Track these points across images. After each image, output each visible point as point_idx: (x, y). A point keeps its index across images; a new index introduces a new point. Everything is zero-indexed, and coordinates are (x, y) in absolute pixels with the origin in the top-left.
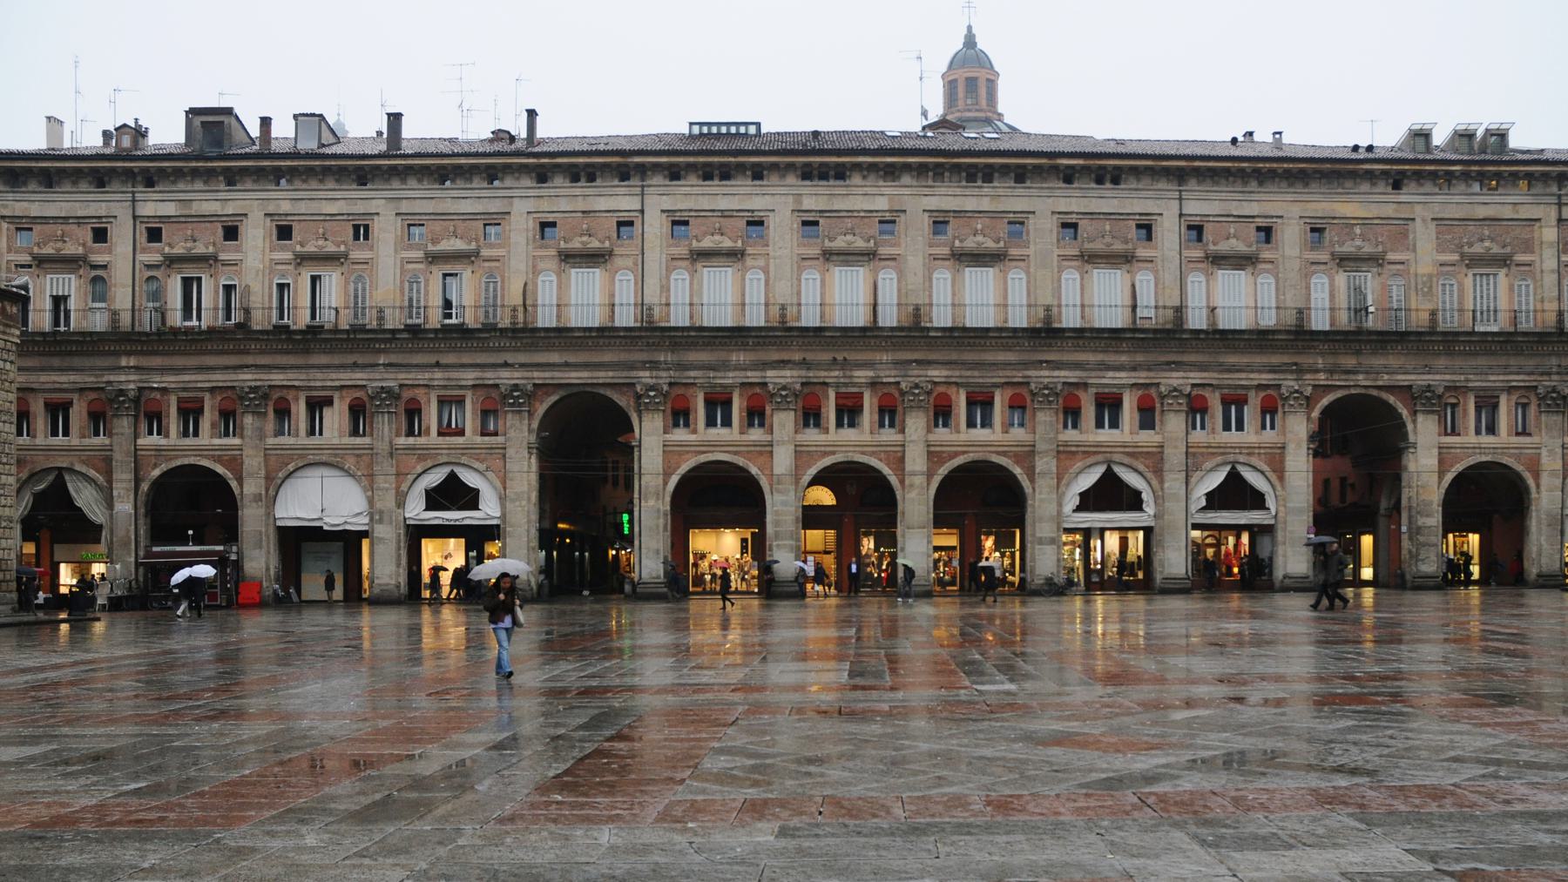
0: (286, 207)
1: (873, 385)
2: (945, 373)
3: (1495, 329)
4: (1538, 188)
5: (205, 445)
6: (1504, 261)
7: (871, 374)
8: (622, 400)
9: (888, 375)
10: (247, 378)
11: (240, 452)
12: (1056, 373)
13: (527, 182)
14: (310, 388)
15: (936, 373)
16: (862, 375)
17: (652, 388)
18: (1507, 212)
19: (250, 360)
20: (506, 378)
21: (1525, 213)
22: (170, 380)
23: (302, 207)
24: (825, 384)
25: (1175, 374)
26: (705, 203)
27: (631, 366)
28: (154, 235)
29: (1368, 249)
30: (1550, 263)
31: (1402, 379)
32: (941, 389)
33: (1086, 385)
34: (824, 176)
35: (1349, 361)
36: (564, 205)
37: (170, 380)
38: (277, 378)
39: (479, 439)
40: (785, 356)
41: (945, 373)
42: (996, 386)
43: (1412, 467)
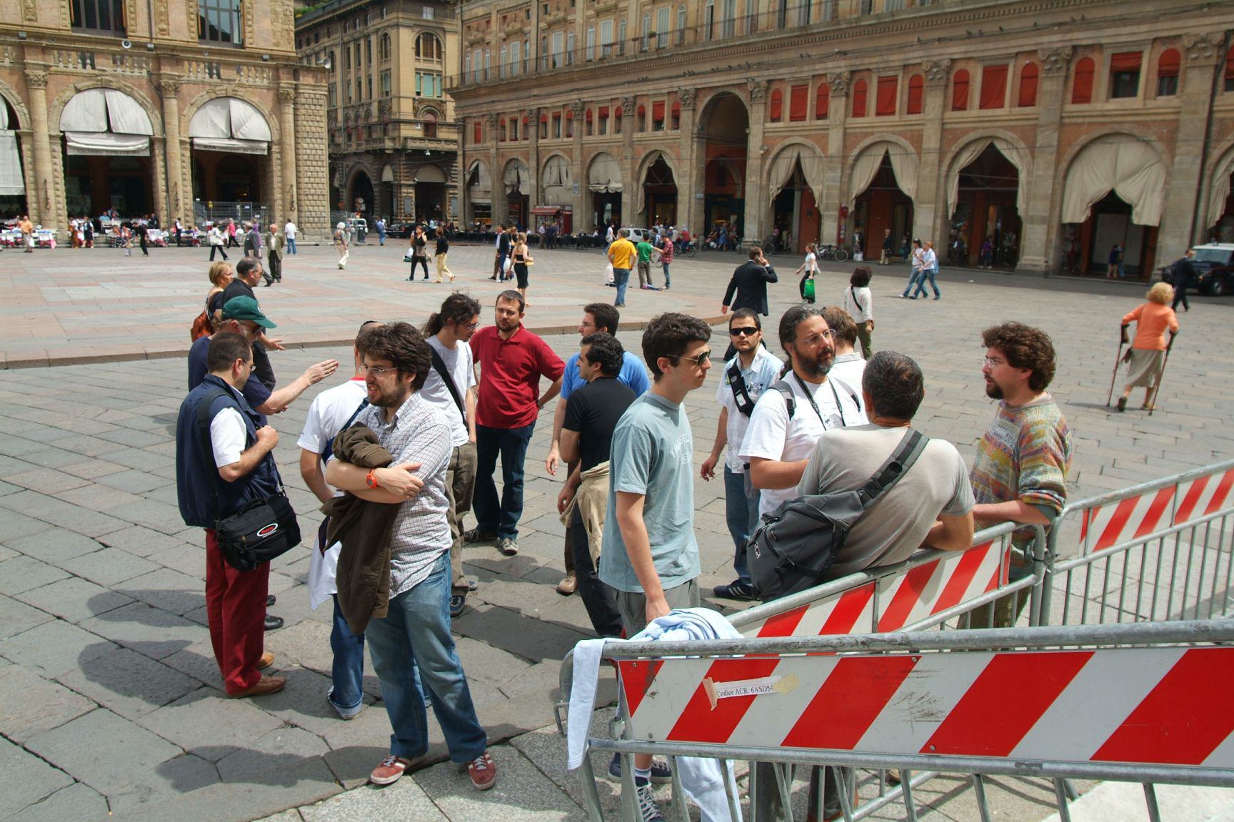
1: (905, 67)
2: (963, 49)
7: (902, 56)
8: (742, 96)
9: (915, 56)
12: (1068, 36)
14: (599, 102)
15: (956, 50)
16: (896, 59)
17: (758, 85)
19: (576, 86)
22: (547, 102)
24: (869, 70)
25: (1207, 21)
27: (749, 67)
32: (959, 66)
33: (1099, 47)
38: (586, 96)
40: (844, 48)
41: (963, 49)
42: (1009, 56)
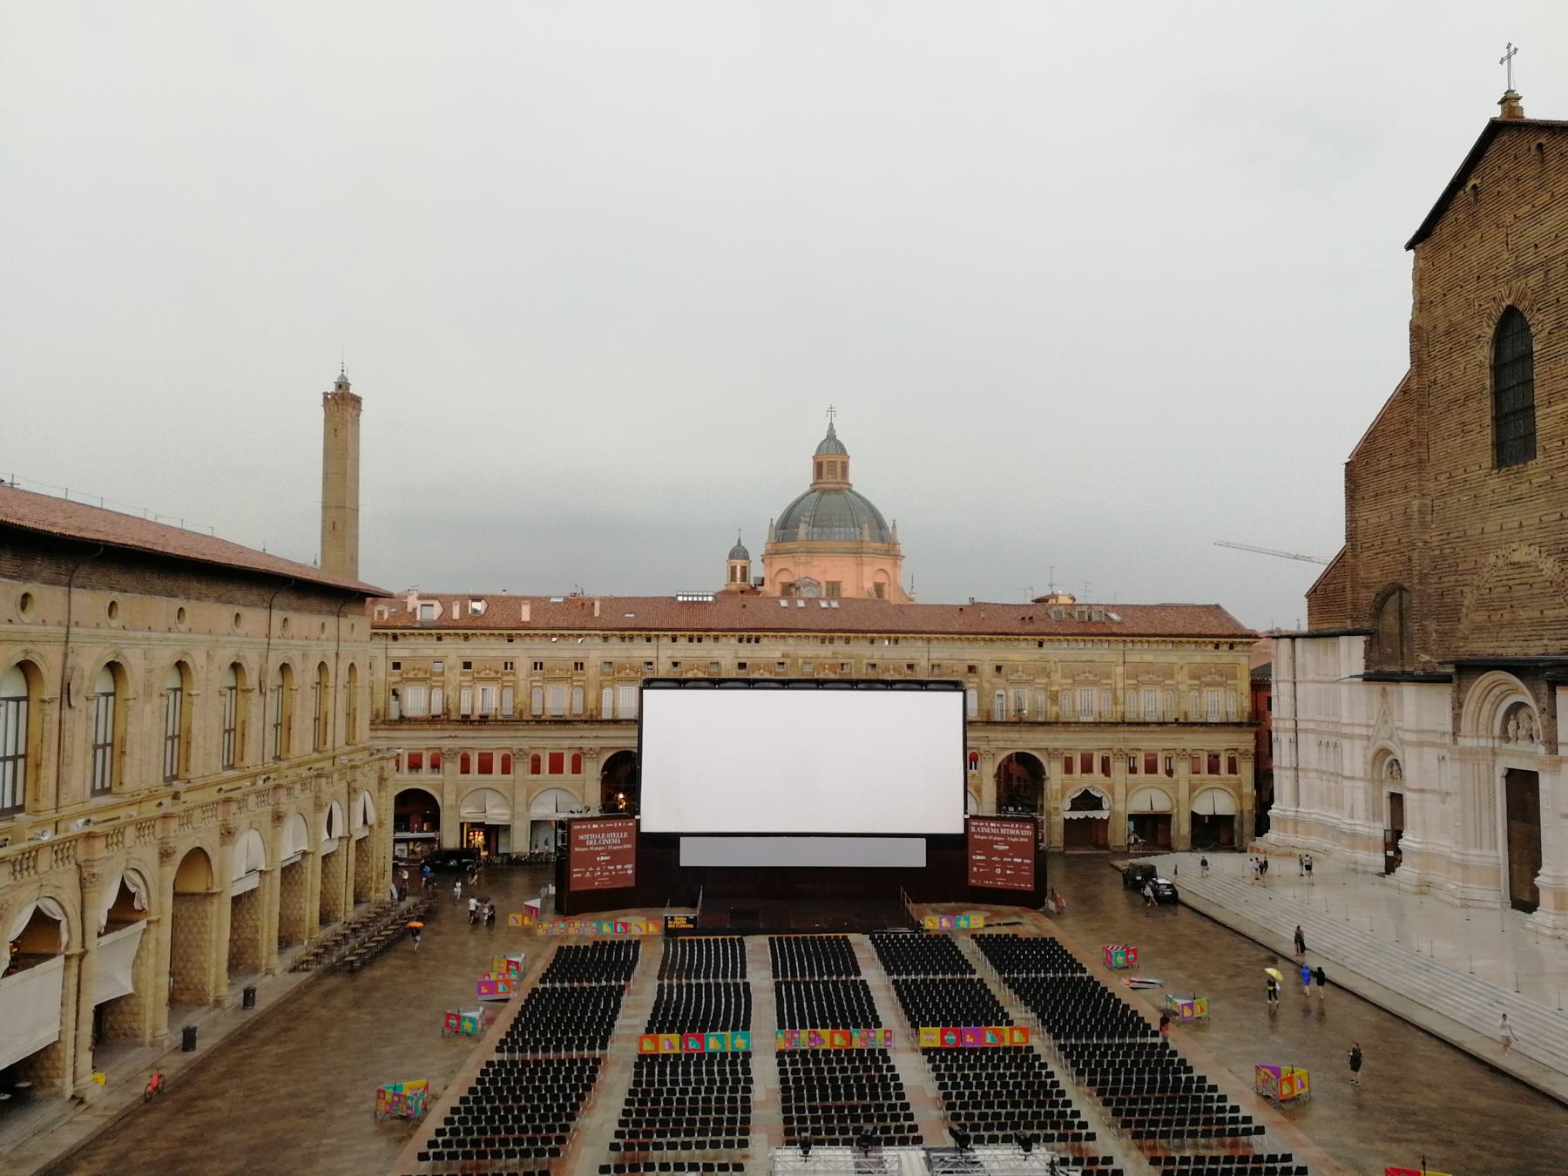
0: (468, 652)
3: (1091, 719)
4: (1114, 645)
5: (424, 780)
6: (1095, 683)
10: (447, 744)
11: (445, 785)
13: (598, 641)
18: (1097, 658)
20: (586, 744)
21: (1106, 659)
23: (478, 653)
26: (689, 653)
28: (397, 666)
29: (1025, 677)
30: (1120, 685)
31: (1043, 745)
34: (749, 641)
35: (1014, 735)
36: (616, 653)
37: (405, 744)
39: (572, 776)
43: (1047, 791)
